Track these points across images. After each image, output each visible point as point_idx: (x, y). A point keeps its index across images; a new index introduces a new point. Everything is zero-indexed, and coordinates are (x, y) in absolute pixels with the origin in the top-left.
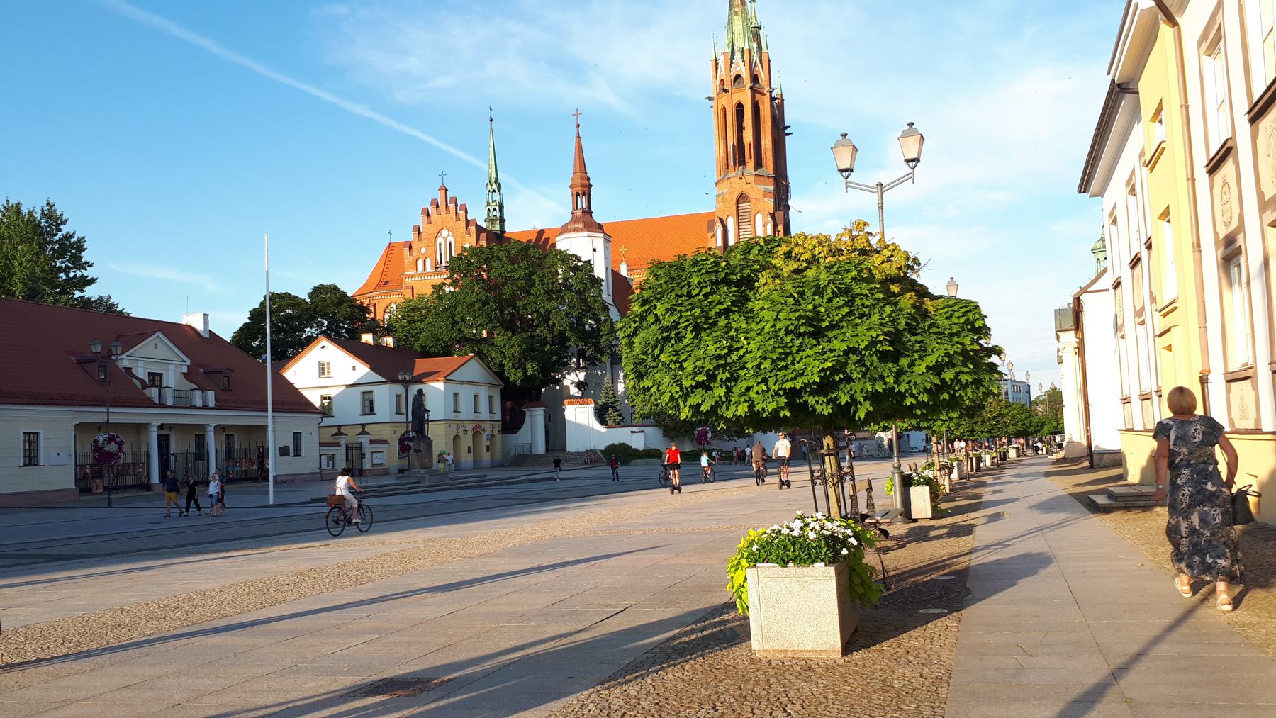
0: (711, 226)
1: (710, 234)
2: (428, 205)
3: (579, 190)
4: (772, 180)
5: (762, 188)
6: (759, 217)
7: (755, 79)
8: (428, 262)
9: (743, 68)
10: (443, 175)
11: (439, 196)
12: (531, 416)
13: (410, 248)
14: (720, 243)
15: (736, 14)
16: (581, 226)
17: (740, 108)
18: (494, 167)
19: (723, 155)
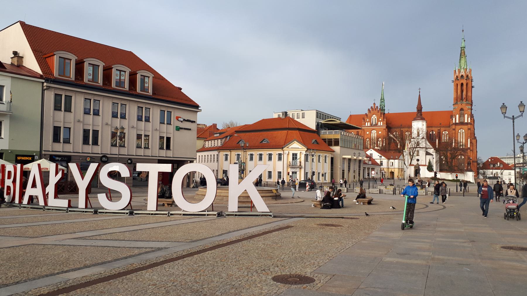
0: (452, 117)
1: (451, 119)
2: (370, 108)
3: (419, 109)
4: (470, 105)
5: (468, 107)
6: (466, 116)
7: (467, 76)
8: (369, 123)
9: (464, 73)
10: (375, 100)
11: (373, 106)
12: (410, 168)
13: (364, 119)
14: (454, 122)
15: (462, 57)
16: (420, 118)
17: (462, 84)
18: (383, 95)
19: (456, 97)
